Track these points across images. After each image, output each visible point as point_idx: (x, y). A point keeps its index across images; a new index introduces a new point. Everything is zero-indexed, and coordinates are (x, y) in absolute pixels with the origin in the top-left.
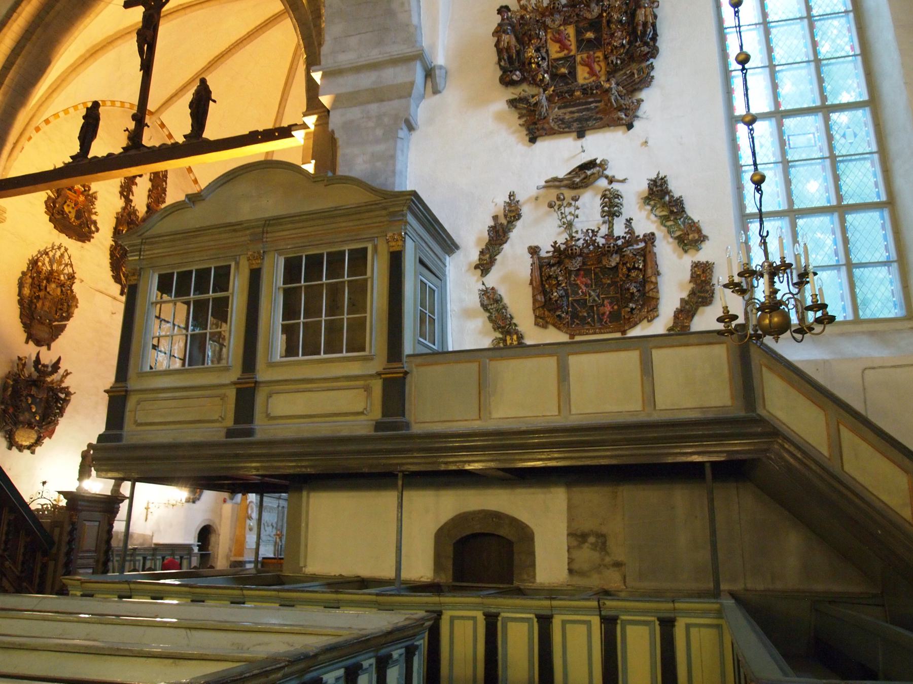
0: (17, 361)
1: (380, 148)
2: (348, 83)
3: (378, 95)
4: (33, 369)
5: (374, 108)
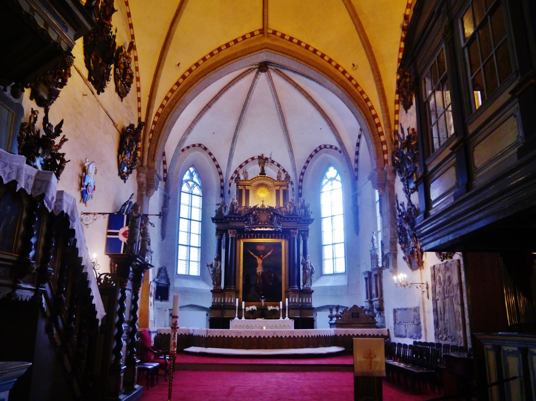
0: (30, 114)
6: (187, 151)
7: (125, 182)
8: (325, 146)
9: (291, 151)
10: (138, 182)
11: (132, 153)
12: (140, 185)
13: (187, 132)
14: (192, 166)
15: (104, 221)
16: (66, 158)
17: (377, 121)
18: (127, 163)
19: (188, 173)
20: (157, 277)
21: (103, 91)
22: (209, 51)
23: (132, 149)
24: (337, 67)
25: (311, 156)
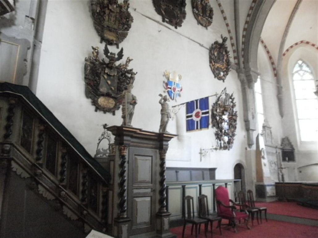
0: (93, 50)
4: (104, 56)
6: (291, 50)
7: (224, 81)
10: (240, 80)
11: (224, 61)
12: (242, 82)
13: (285, 35)
14: (301, 59)
15: (184, 109)
16: (134, 71)
18: (221, 68)
19: (297, 65)
20: (281, 145)
21: (180, 26)
23: (223, 58)
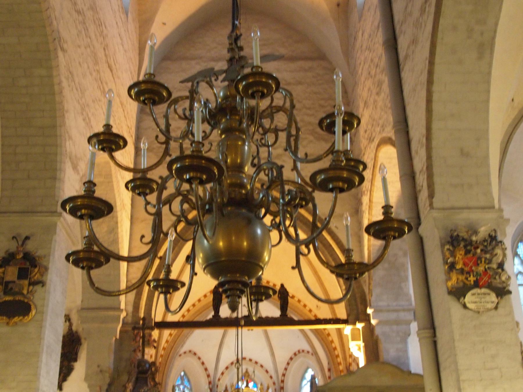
1: (400, 346)
2: (385, 316)
3: (397, 322)
5: (395, 327)
8: (303, 351)
9: (273, 354)
17: (336, 353)
22: (203, 294)
24: (305, 306)
25: (291, 359)
